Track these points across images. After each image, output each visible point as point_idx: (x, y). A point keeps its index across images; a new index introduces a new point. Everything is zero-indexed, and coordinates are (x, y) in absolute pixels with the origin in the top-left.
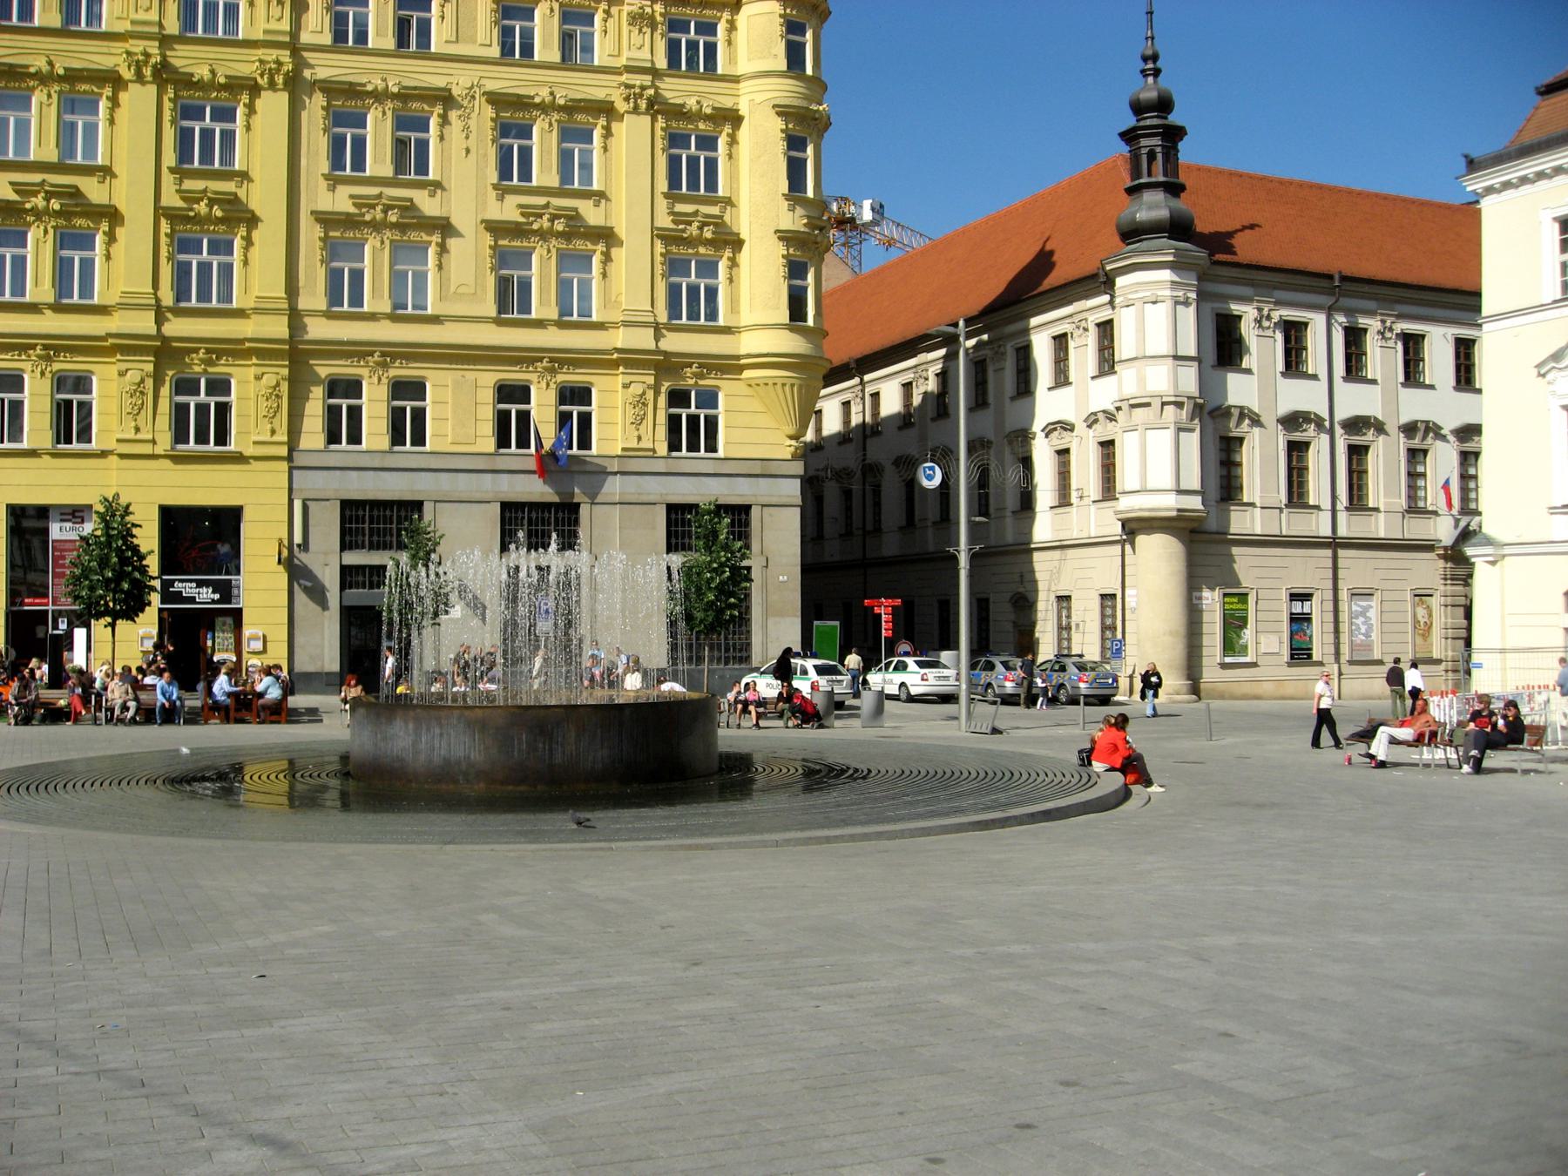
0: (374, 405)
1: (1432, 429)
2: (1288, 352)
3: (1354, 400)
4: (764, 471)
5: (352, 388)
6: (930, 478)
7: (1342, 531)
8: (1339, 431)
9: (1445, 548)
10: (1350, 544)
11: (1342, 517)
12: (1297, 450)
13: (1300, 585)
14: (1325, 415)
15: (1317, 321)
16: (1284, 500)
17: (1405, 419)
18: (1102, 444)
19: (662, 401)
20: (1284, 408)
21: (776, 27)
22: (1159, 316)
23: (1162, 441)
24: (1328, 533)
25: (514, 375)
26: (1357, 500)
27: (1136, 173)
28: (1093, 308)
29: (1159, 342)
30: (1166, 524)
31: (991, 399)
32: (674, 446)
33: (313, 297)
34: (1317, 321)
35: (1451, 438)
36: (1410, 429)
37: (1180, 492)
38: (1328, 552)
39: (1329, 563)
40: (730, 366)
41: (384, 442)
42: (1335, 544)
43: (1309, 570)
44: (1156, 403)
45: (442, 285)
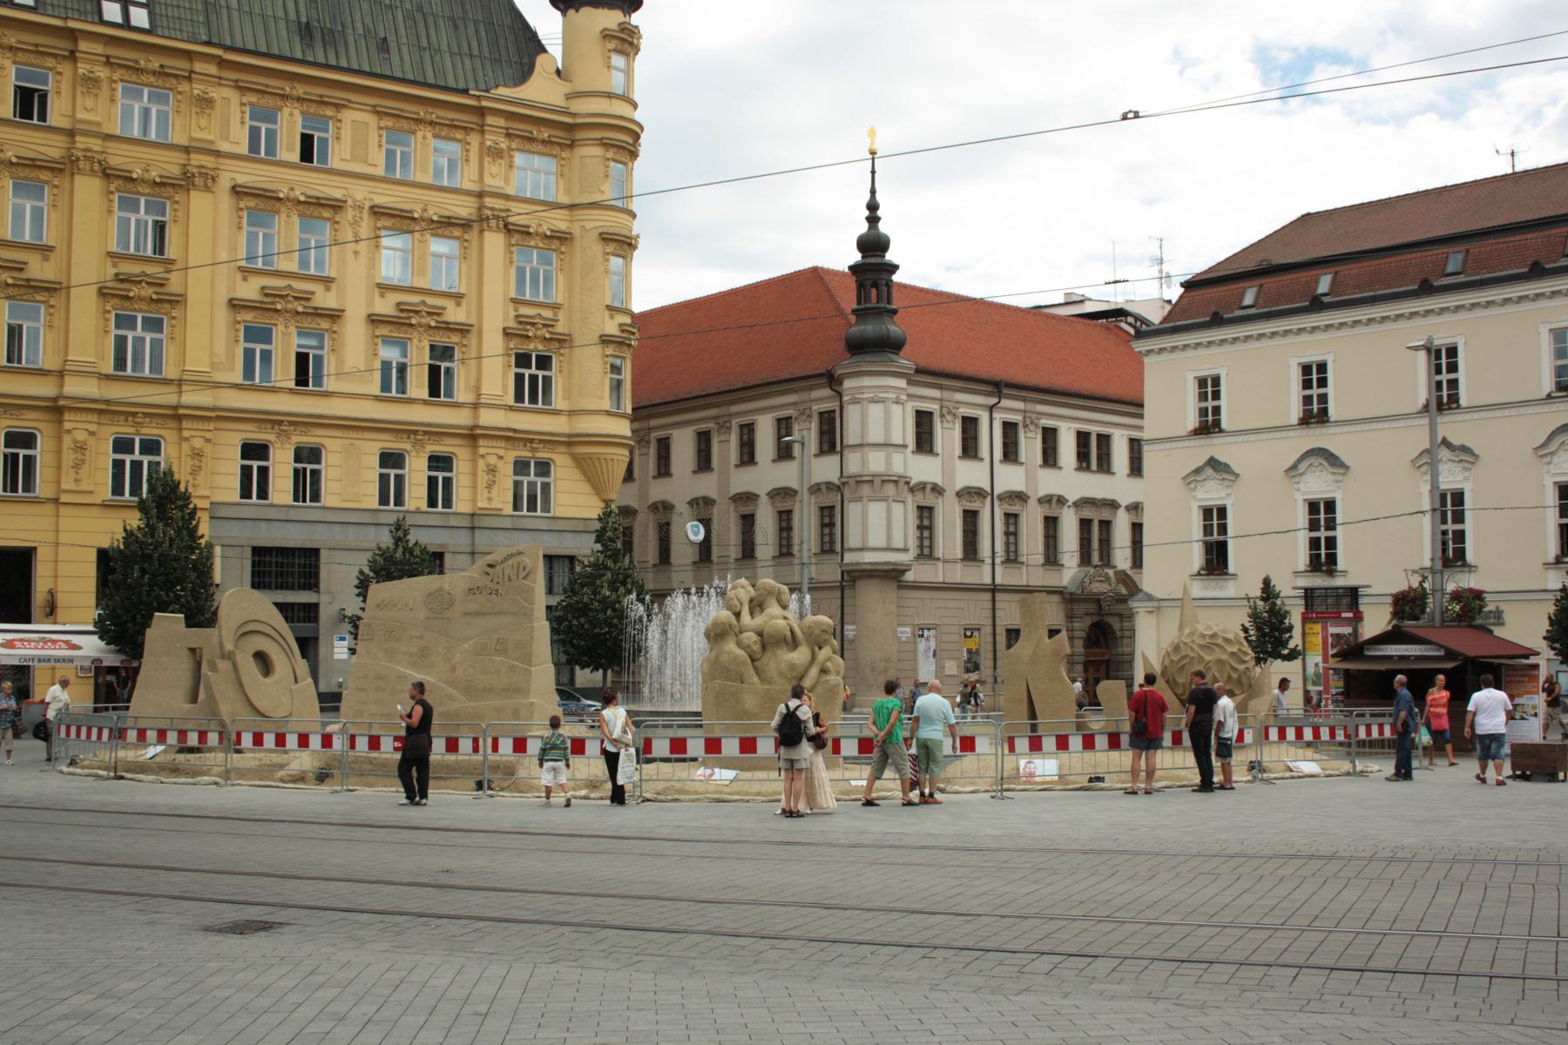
0: (282, 466)
1: (1061, 501)
2: (965, 440)
3: (1010, 478)
6: (696, 534)
7: (998, 581)
10: (1007, 589)
11: (998, 569)
12: (970, 517)
13: (972, 621)
14: (988, 489)
16: (960, 555)
17: (1041, 493)
18: (822, 509)
20: (959, 486)
25: (394, 445)
26: (1012, 558)
28: (821, 399)
31: (715, 463)
34: (984, 416)
36: (1047, 500)
39: (989, 605)
42: (994, 590)
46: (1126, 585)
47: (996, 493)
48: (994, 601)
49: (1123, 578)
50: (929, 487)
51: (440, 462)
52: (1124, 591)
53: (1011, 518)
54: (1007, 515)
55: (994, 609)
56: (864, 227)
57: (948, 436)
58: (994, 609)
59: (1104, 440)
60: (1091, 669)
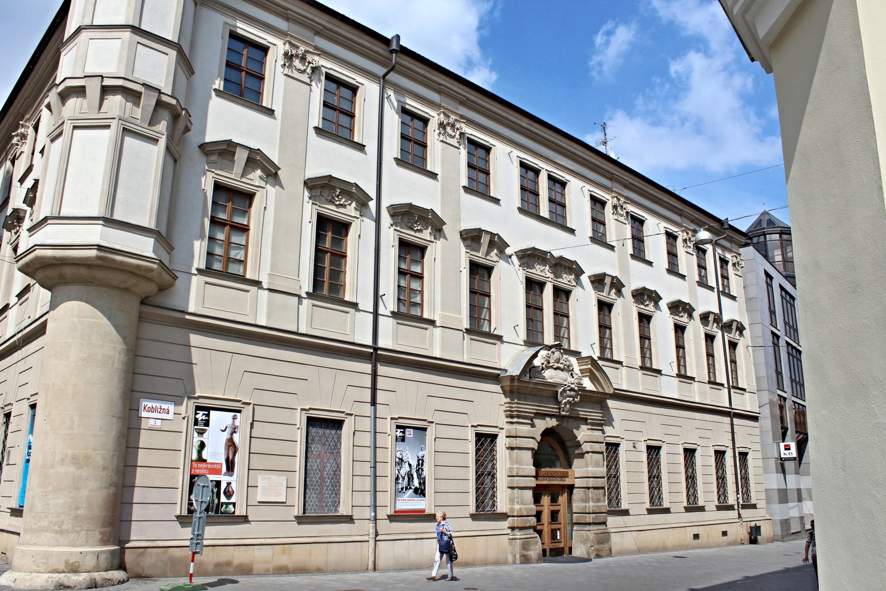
1: (498, 244)
8: (386, 219)
9: (512, 378)
11: (386, 324)
13: (326, 406)
14: (373, 194)
15: (369, 91)
16: (307, 285)
20: (314, 171)
24: (369, 342)
30: (84, 271)
34: (369, 91)
35: (514, 258)
37: (109, 222)
38: (367, 367)
42: (375, 356)
43: (336, 387)
44: (93, 89)
46: (593, 378)
47: (385, 204)
48: (374, 375)
49: (594, 369)
50: (241, 157)
52: (588, 384)
53: (410, 250)
54: (404, 245)
55: (374, 389)
58: (374, 389)
59: (557, 183)
60: (546, 500)
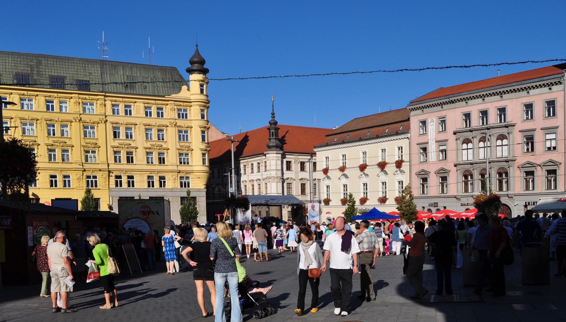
0: (124, 180)
2: (301, 167)
4: (199, 190)
5: (120, 177)
19: (179, 179)
21: (199, 111)
22: (273, 162)
23: (274, 185)
27: (270, 136)
29: (273, 167)
32: (181, 186)
33: (112, 161)
40: (192, 172)
41: (126, 186)
45: (136, 159)
51: (162, 178)
56: (271, 119)
57: (295, 167)
